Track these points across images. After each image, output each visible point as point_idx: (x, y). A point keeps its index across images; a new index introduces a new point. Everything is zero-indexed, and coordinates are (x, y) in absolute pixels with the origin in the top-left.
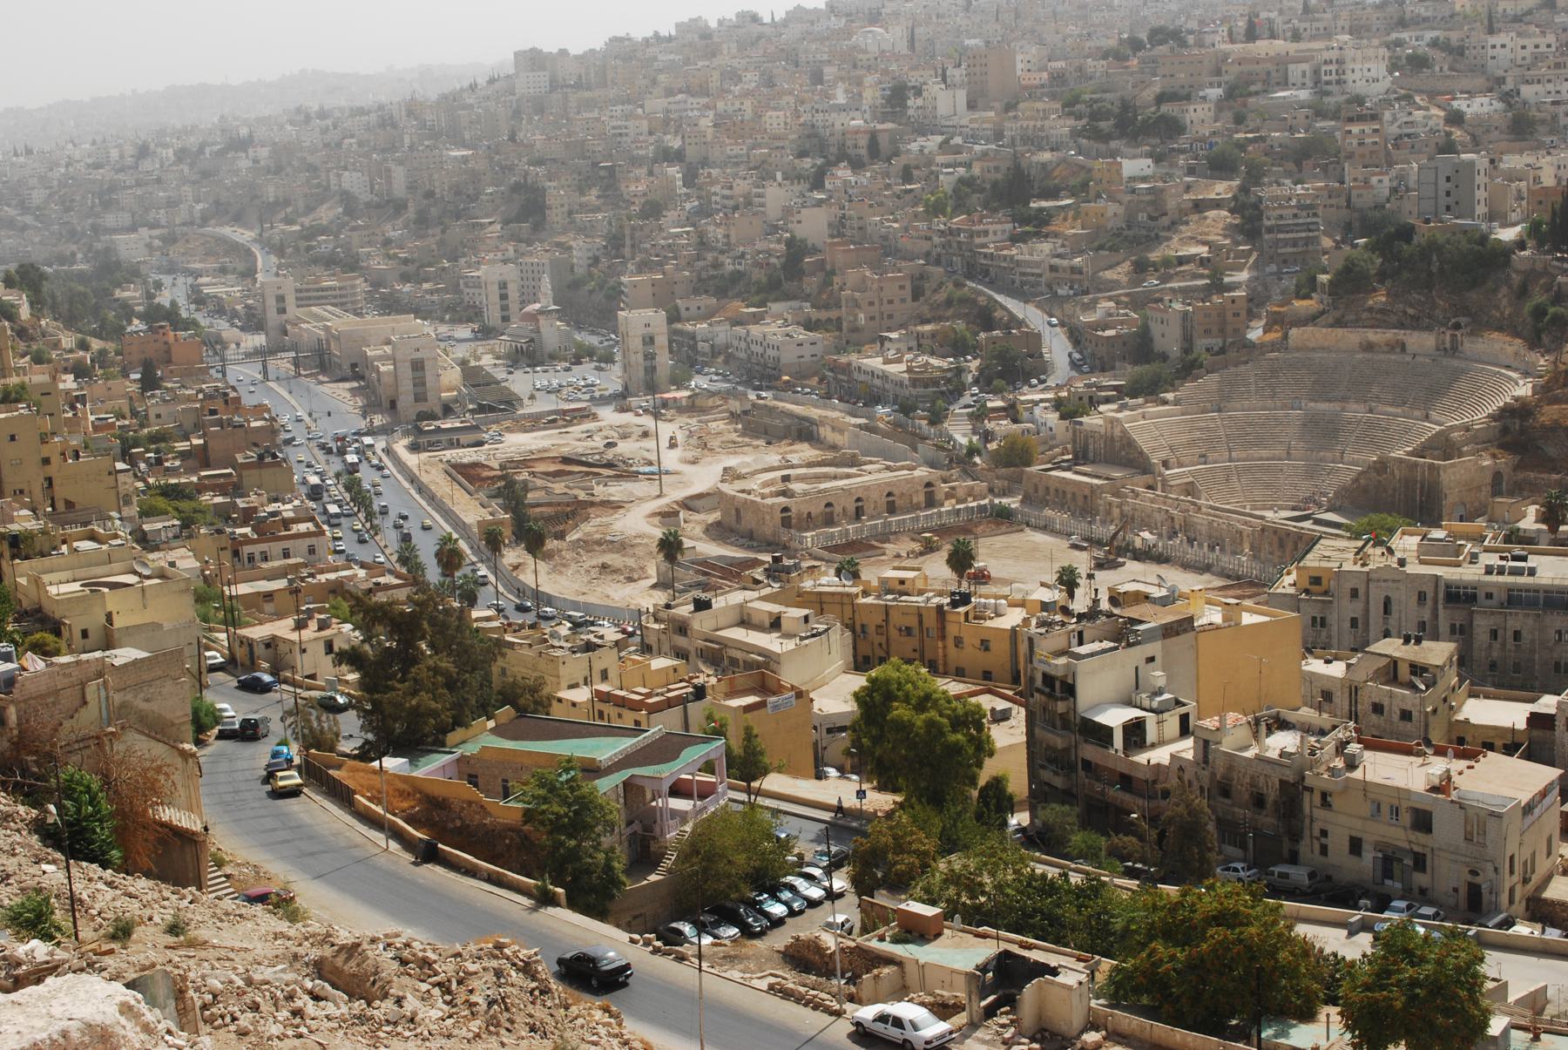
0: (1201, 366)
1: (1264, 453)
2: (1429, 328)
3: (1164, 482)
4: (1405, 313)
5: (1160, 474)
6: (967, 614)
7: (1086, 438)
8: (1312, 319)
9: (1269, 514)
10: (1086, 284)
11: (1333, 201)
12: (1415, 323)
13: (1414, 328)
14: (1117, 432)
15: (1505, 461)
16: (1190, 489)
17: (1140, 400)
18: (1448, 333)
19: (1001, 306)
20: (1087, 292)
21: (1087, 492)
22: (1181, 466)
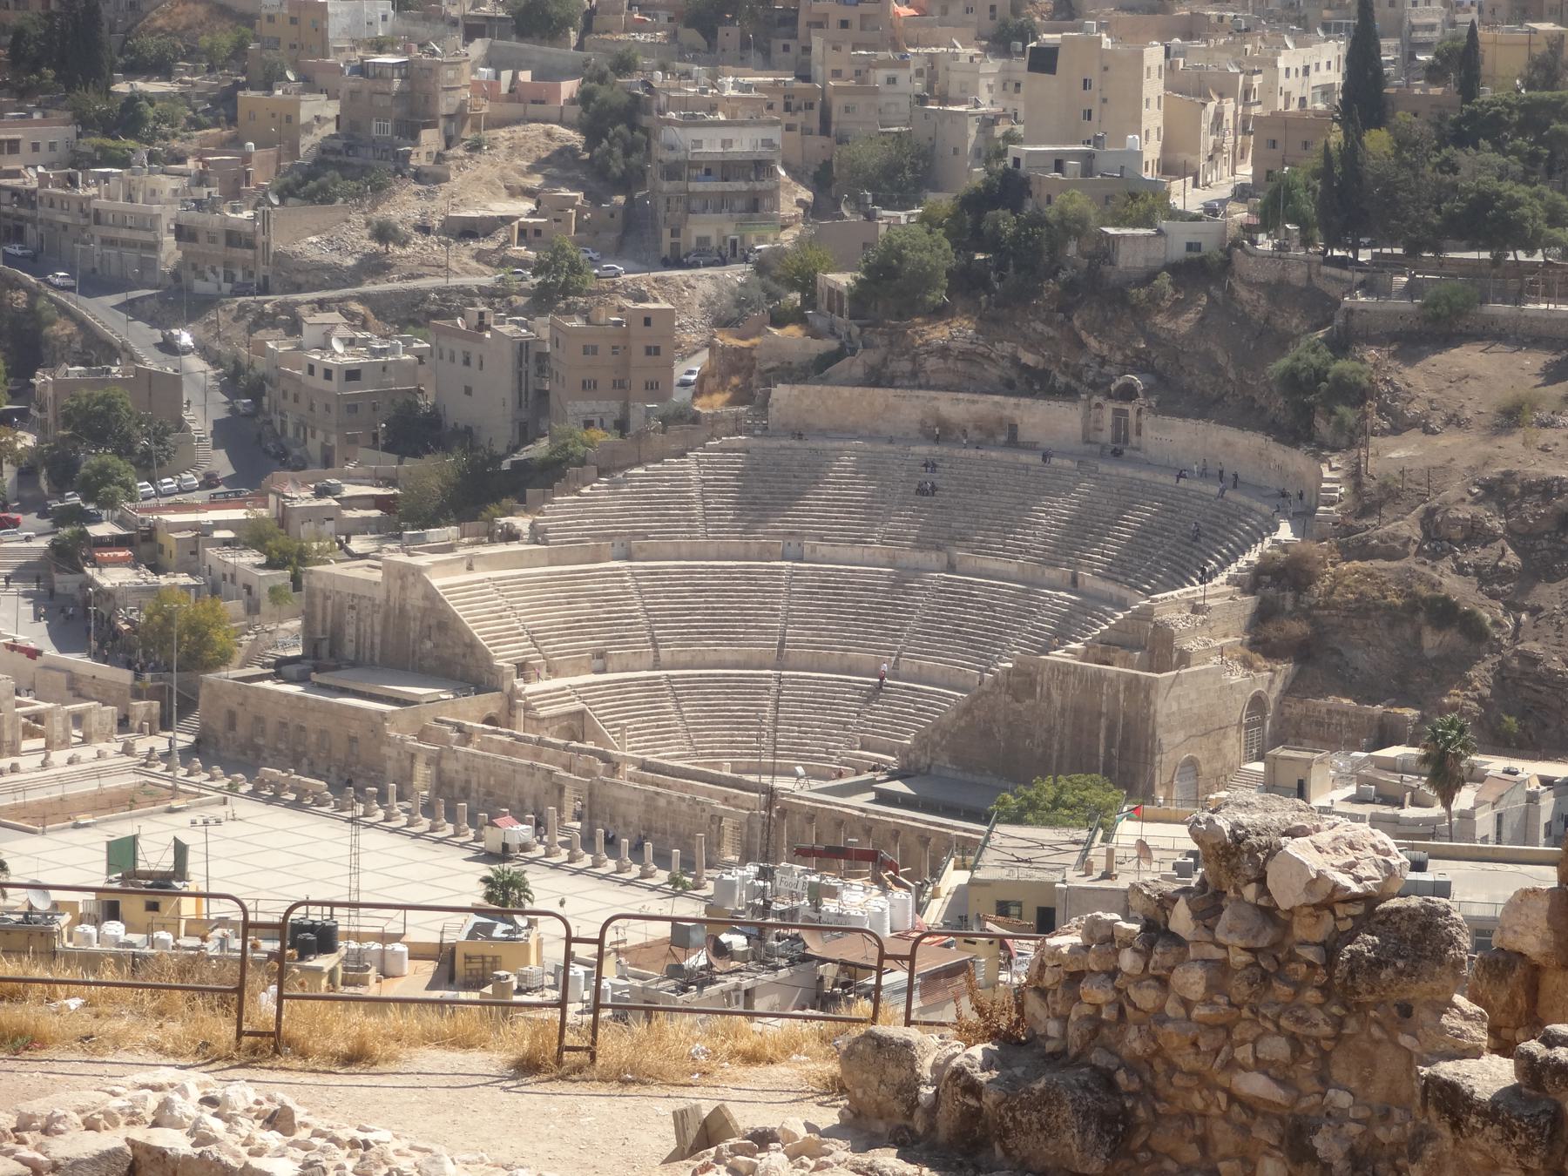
0: (583, 462)
1: (727, 652)
2: (1069, 394)
3: (527, 707)
4: (1015, 360)
5: (513, 694)
6: (333, 972)
8: (818, 369)
9: (782, 783)
10: (262, 270)
11: (799, 119)
12: (1034, 383)
13: (1031, 394)
14: (415, 598)
15: (1270, 678)
16: (577, 725)
17: (451, 531)
18: (1110, 406)
19: (65, 311)
20: (264, 289)
21: (355, 729)
22: (553, 671)
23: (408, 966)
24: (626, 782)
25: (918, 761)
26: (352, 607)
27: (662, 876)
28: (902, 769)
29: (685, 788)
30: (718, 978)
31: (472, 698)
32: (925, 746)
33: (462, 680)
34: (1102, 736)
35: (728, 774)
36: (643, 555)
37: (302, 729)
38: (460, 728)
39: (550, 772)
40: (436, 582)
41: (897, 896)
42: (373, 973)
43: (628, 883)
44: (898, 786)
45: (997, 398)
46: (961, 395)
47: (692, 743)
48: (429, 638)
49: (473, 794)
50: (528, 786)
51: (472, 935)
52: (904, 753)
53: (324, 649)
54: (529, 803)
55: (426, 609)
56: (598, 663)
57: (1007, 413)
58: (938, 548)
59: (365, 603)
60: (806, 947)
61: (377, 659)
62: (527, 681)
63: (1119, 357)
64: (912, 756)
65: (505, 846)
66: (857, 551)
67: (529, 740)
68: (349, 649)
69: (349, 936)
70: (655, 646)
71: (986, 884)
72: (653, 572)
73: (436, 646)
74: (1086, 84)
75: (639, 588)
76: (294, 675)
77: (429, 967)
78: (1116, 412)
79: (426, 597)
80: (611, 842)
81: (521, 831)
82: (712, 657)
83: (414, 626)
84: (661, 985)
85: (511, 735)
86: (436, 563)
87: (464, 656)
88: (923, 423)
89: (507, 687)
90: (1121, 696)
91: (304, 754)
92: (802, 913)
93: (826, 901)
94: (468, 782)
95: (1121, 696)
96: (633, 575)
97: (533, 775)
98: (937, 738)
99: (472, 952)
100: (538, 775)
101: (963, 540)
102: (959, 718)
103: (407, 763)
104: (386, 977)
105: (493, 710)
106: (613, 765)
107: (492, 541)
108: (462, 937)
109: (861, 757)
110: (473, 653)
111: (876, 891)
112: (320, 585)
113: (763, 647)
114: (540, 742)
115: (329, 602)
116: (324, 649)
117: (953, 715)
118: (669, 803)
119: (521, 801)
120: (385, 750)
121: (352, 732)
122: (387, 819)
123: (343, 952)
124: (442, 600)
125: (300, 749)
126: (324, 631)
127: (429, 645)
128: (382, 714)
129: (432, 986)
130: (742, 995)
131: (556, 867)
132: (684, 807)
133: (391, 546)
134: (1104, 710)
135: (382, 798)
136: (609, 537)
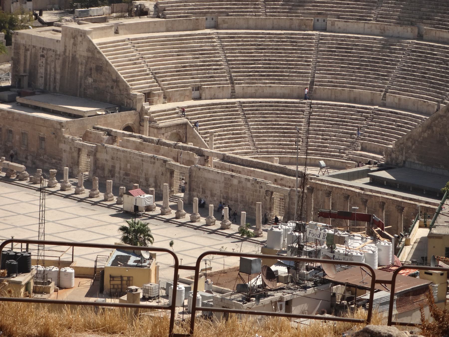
1: (278, 88)
3: (151, 121)
5: (143, 112)
6: (28, 284)
7: (36, 56)
14: (82, 51)
16: (182, 133)
17: (105, 9)
21: (44, 132)
22: (167, 98)
23: (75, 281)
24: (213, 169)
25: (397, 159)
26: (43, 56)
27: (234, 228)
28: (387, 163)
29: (250, 173)
30: (269, 293)
31: (117, 114)
32: (402, 149)
33: (111, 102)
35: (277, 164)
36: (225, 25)
37: (10, 131)
38: (109, 133)
39: (165, 161)
40: (95, 41)
41: (383, 244)
42: (53, 286)
43: (213, 232)
44: (384, 174)
47: (254, 145)
48: (90, 75)
49: (117, 175)
50: (152, 170)
51: (115, 263)
52: (388, 153)
53: (25, 81)
54: (151, 181)
55: (88, 58)
56: (196, 93)
58: (412, 24)
59: (50, 53)
60: (325, 274)
61: (57, 89)
62: (151, 103)
64: (394, 156)
65: (136, 208)
66: (361, 24)
67: (152, 141)
68: (40, 82)
69: (38, 262)
70: (232, 83)
71: (439, 237)
72: (232, 37)
73: (95, 81)
75: (223, 46)
76: (6, 98)
77: (87, 283)
79: (89, 50)
80: (203, 207)
81: (145, 199)
82: (268, 91)
83: (82, 68)
84: (233, 297)
85: (141, 138)
86: (95, 29)
87: (112, 88)
89: (139, 109)
91: (12, 148)
92: (323, 253)
93: (338, 246)
94: (114, 167)
96: (219, 38)
97: (154, 163)
98: (410, 144)
99: (115, 273)
100: (158, 164)
101: (428, 19)
102: (423, 132)
103: (75, 154)
104: (61, 288)
105: (130, 122)
106: (204, 157)
107: (131, 16)
108: (108, 264)
109: (361, 155)
110: (118, 86)
111: (369, 241)
112: (22, 42)
113: (300, 84)
114: (159, 143)
115: (29, 53)
116: (25, 81)
117: (420, 130)
118: (240, 182)
119: (147, 180)
120: (62, 146)
121: (42, 134)
122: (62, 189)
123: (34, 272)
124: (99, 52)
125: (9, 144)
126: (25, 71)
127: (90, 80)
128: (60, 123)
129: (89, 294)
130: (284, 304)
131: (167, 221)
132: (249, 185)
133: (68, 18)
135: (60, 176)
136: (205, 14)
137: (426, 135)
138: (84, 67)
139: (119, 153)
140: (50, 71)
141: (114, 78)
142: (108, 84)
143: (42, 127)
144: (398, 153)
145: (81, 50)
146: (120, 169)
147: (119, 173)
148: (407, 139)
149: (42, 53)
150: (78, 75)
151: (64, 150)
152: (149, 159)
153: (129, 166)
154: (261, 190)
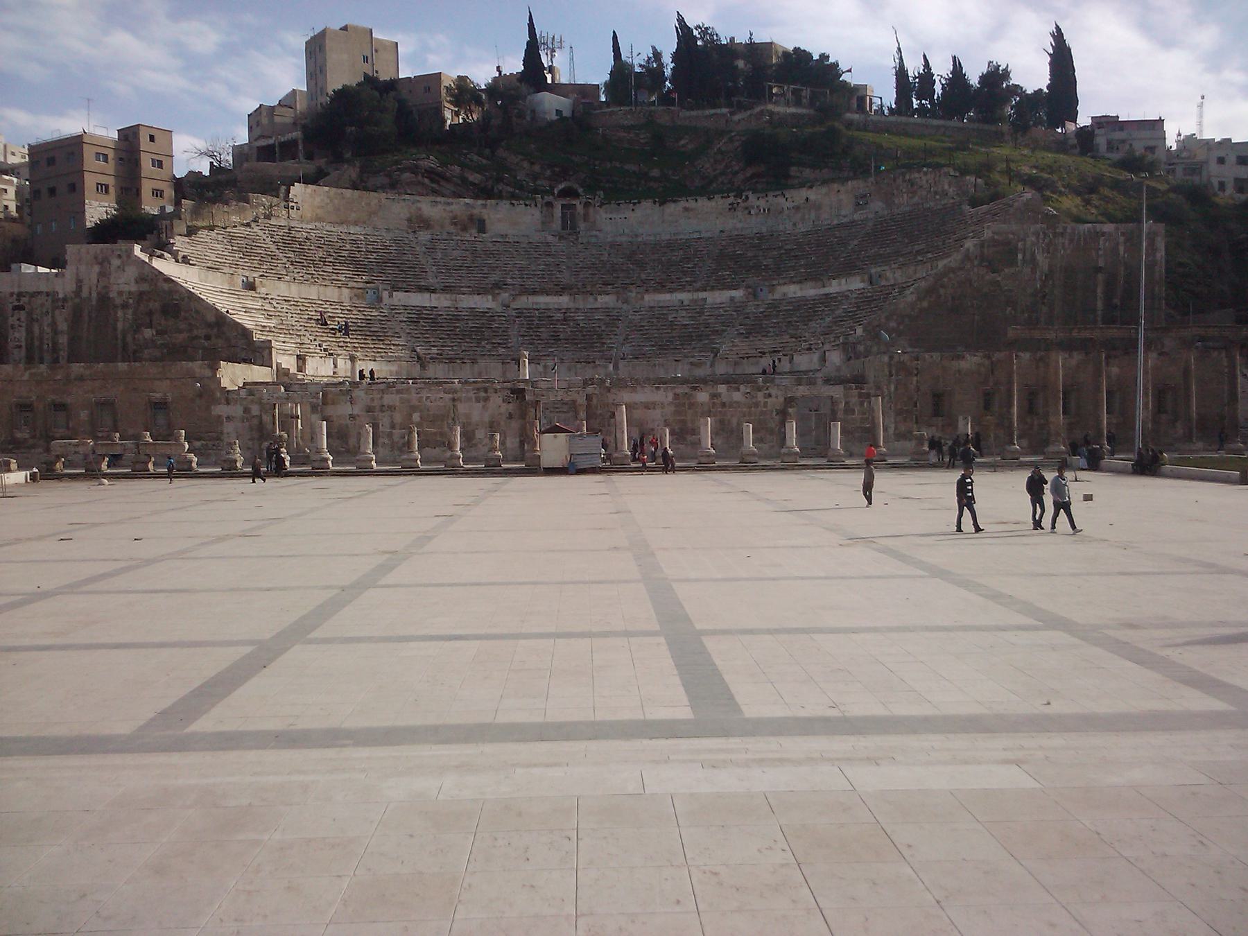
4: (464, 180)
34: (1099, 290)
37: (60, 407)
45: (467, 200)
46: (439, 199)
55: (141, 294)
57: (476, 211)
63: (548, 173)
74: (366, 59)
78: (563, 206)
79: (141, 279)
83: (123, 319)
88: (409, 220)
90: (1121, 249)
95: (1121, 249)
97: (486, 399)
100: (496, 400)
102: (919, 299)
120: (221, 410)
127: (148, 333)
134: (1101, 264)
137: (925, 304)
138: (130, 311)
139: (386, 396)
140: (42, 332)
141: (211, 318)
142: (195, 332)
143: (157, 383)
144: (869, 343)
145: (120, 281)
146: (393, 426)
147: (390, 435)
148: (887, 318)
149: (16, 303)
150: (115, 329)
151: (228, 418)
152: (471, 394)
153: (416, 417)
154: (769, 400)
